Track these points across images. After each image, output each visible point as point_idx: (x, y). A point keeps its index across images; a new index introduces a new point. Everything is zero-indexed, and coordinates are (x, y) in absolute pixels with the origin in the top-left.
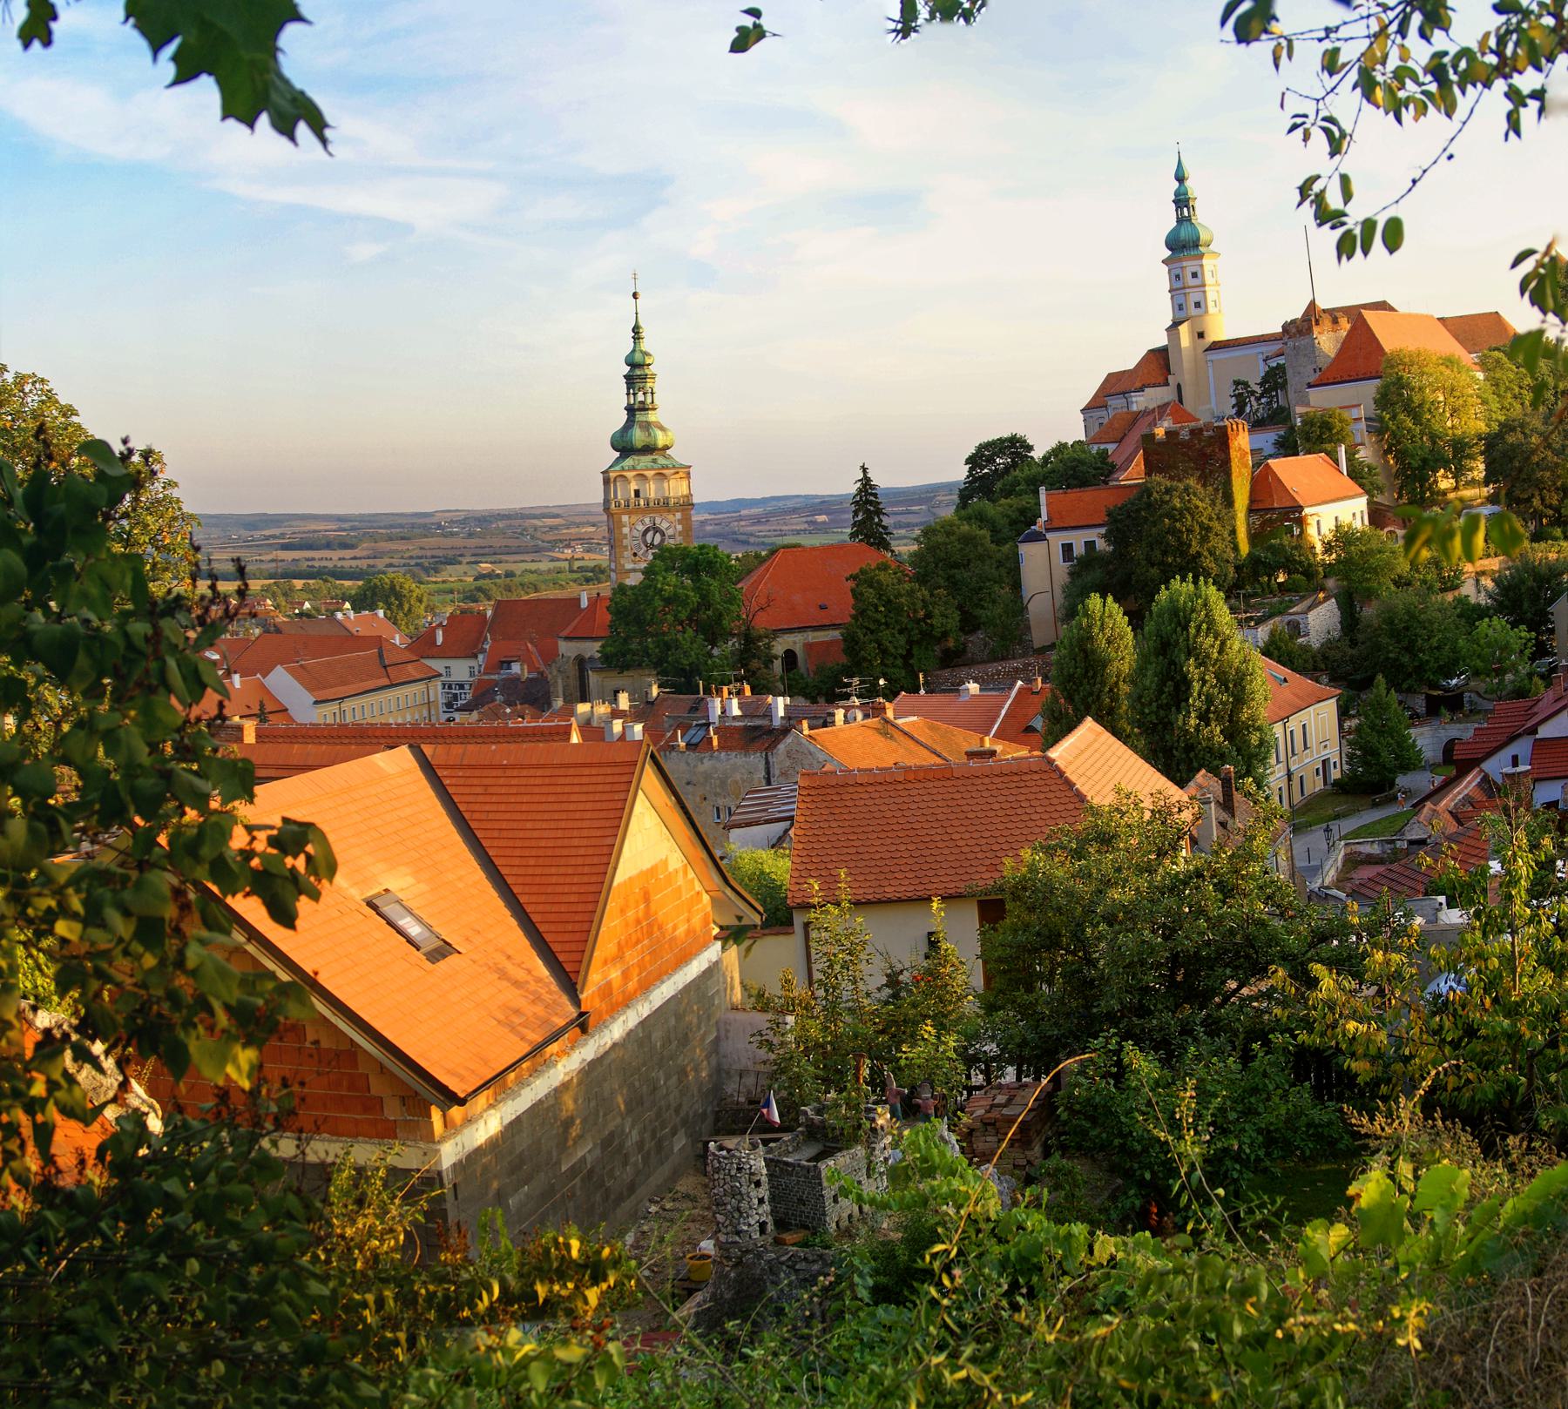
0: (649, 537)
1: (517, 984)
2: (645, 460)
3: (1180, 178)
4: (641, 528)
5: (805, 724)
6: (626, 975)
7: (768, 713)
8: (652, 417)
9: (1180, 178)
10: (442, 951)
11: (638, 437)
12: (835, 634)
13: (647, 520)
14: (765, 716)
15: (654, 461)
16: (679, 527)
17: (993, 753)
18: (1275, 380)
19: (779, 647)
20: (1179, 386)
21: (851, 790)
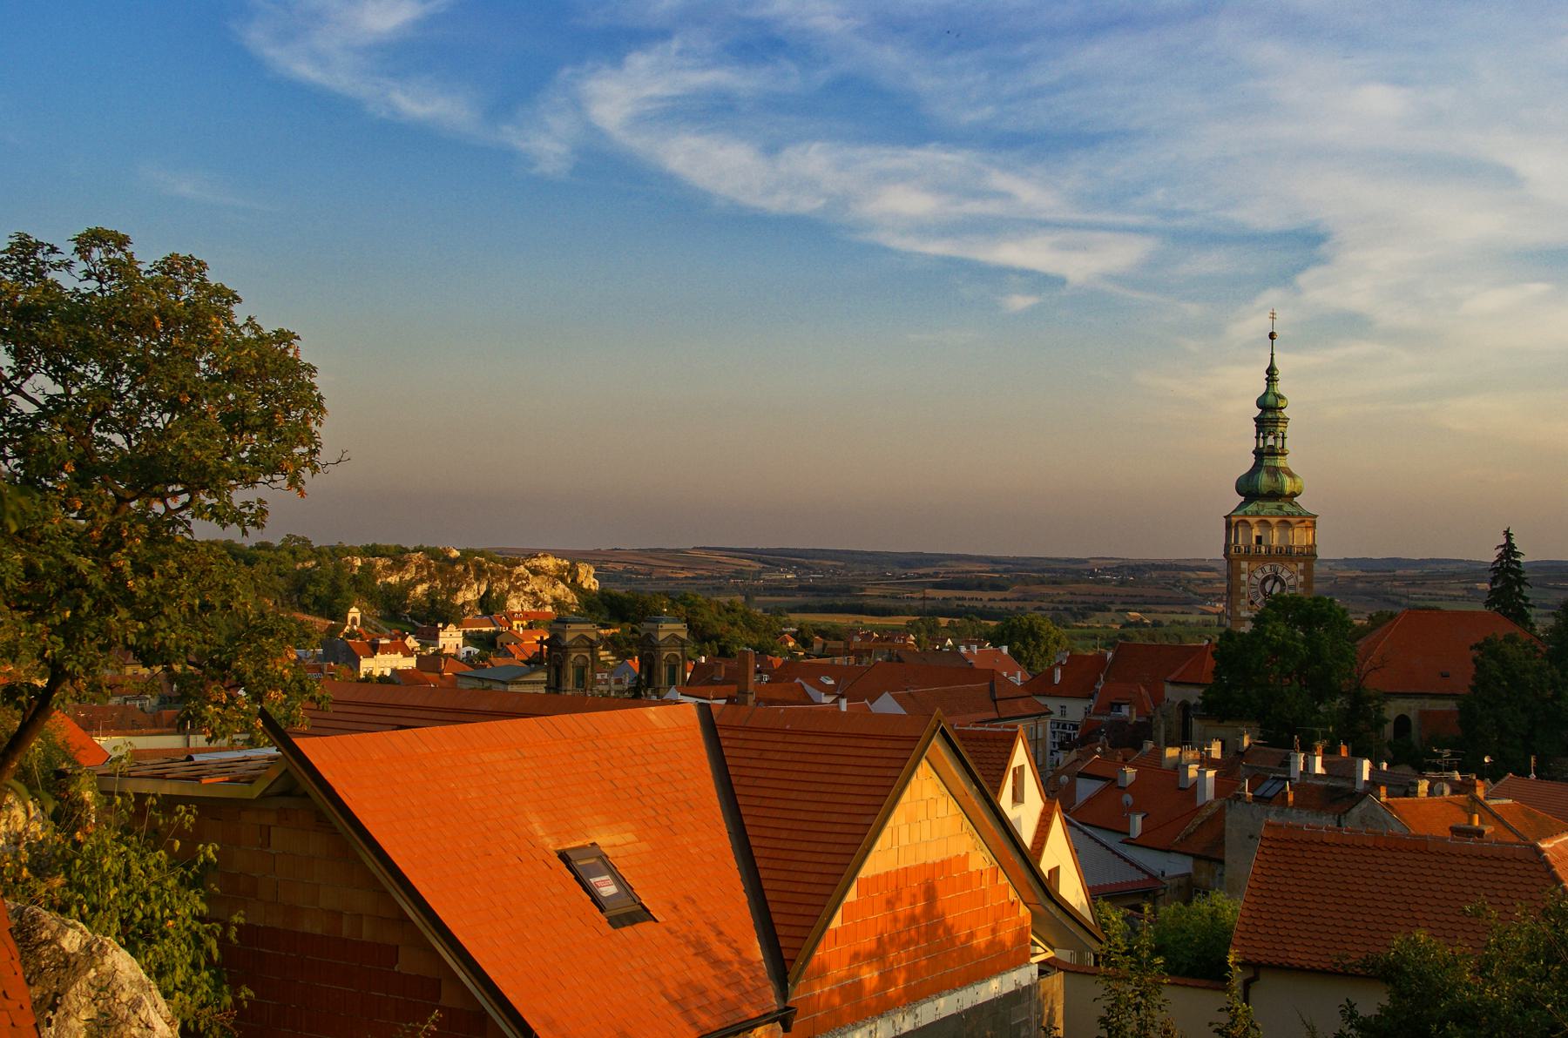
1: (716, 963)
2: (1270, 506)
4: (1260, 575)
5: (1383, 790)
6: (886, 978)
7: (1352, 774)
8: (1281, 462)
10: (641, 914)
11: (1264, 480)
12: (1450, 705)
13: (1267, 568)
14: (1343, 777)
15: (1280, 508)
17: (1480, 833)
19: (1392, 710)
21: (1315, 848)
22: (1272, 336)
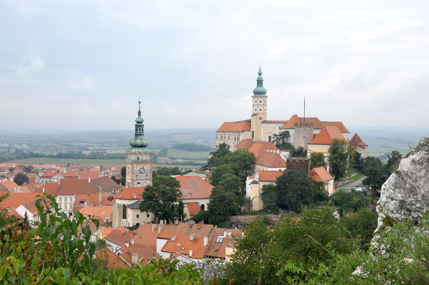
0: (141, 170)
3: (260, 74)
4: (139, 168)
9: (260, 74)
13: (141, 166)
16: (149, 168)
18: (285, 135)
20: (253, 132)
22: (140, 103)
